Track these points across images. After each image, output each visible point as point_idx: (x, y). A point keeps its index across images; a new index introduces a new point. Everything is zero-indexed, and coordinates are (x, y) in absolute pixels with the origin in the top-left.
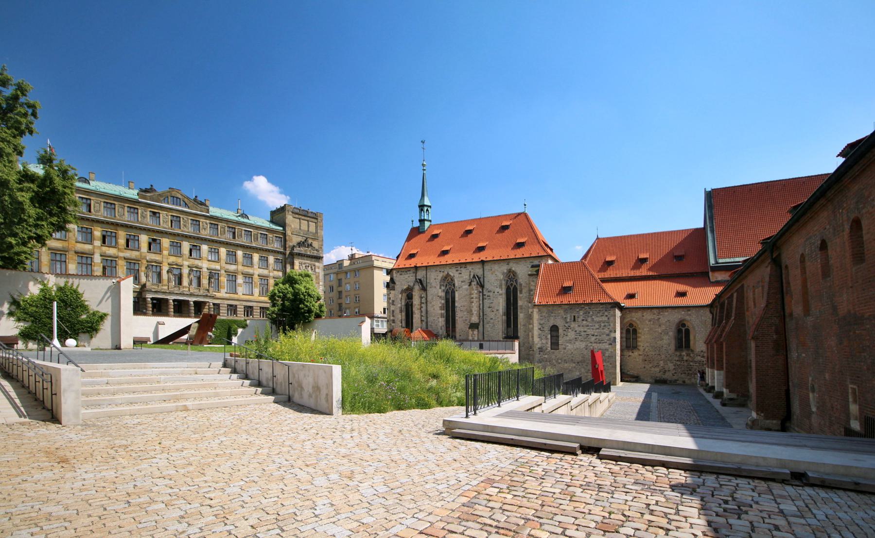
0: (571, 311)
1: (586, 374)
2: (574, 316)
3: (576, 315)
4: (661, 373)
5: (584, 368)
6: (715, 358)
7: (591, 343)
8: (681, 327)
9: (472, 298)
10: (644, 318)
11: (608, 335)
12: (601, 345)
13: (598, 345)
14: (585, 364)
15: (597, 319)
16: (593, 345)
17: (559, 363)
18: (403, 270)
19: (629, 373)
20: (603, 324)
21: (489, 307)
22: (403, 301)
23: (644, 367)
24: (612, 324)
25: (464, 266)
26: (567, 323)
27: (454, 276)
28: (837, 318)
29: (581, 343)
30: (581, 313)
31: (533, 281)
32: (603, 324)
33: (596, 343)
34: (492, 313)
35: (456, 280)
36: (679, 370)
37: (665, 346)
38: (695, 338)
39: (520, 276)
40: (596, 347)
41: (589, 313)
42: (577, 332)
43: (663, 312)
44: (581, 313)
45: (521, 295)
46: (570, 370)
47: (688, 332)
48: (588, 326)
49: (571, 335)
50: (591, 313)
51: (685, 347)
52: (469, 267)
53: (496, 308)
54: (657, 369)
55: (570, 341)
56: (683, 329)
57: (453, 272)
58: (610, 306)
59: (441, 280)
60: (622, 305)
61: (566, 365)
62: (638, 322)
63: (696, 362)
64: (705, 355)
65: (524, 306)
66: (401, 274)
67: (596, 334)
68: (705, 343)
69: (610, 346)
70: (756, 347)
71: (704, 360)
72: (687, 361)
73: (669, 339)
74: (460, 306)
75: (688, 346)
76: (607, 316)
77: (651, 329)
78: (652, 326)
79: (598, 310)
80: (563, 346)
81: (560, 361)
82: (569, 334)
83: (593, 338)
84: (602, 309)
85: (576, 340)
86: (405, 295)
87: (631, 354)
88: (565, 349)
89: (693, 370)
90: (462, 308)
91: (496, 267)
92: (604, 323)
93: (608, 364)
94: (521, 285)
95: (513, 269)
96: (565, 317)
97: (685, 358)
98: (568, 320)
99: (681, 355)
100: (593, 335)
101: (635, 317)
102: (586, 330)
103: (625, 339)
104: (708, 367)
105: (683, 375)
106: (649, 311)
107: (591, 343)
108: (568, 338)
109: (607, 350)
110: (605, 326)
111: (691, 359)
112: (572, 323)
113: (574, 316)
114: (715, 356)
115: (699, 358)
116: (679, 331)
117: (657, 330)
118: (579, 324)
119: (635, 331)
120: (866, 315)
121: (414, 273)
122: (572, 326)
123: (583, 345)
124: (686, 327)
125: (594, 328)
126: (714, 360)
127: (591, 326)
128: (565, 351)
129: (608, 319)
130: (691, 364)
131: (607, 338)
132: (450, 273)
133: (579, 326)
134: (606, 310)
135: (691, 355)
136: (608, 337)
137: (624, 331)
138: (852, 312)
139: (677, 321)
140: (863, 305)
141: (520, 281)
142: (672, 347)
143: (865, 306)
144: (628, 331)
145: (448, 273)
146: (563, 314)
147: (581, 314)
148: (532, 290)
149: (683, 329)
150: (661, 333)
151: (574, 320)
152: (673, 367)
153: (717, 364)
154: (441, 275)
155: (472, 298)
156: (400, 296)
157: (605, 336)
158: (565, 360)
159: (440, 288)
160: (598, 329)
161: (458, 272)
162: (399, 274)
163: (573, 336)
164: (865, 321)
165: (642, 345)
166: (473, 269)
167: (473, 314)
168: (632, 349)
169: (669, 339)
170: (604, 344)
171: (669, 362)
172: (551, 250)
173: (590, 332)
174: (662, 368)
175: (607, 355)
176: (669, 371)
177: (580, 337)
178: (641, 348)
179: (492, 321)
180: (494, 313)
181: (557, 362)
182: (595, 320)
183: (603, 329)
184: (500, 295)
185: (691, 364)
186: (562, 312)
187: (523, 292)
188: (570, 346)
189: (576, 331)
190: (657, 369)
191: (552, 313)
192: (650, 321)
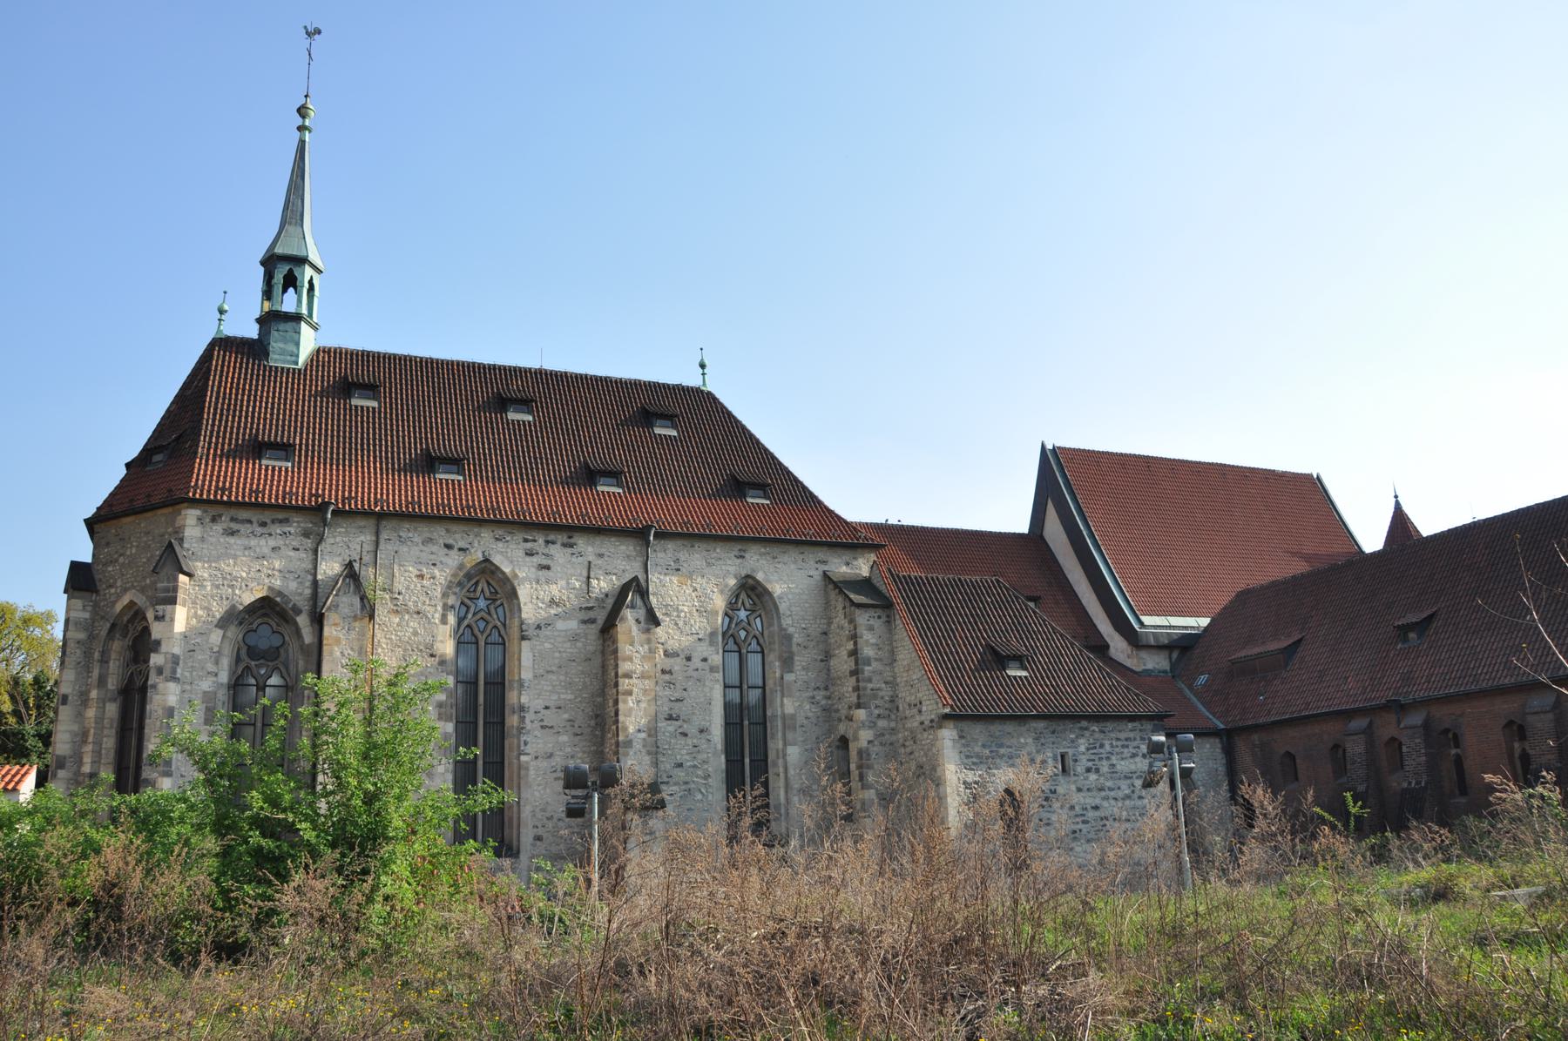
2: (1063, 756)
3: (1070, 752)
9: (628, 676)
18: (243, 514)
21: (670, 718)
22: (225, 662)
25: (561, 538)
27: (516, 576)
29: (1088, 847)
31: (871, 628)
34: (682, 741)
35: (524, 592)
39: (783, 607)
41: (1102, 746)
42: (1077, 808)
45: (789, 677)
48: (1101, 790)
50: (1108, 747)
52: (587, 547)
53: (698, 721)
57: (510, 556)
59: (449, 587)
65: (800, 720)
66: (232, 533)
74: (538, 704)
79: (1123, 735)
82: (1054, 818)
84: (1132, 735)
85: (1075, 839)
86: (234, 632)
90: (551, 718)
91: (695, 557)
94: (788, 638)
95: (760, 576)
102: (1098, 801)
112: (1060, 778)
121: (306, 534)
122: (1060, 790)
127: (1111, 789)
132: (497, 560)
133: (1079, 790)
141: (786, 622)
145: (487, 560)
147: (1082, 749)
148: (868, 662)
151: (1064, 770)
154: (454, 559)
155: (628, 676)
156: (216, 636)
159: (444, 621)
160: (1128, 797)
161: (535, 559)
162: (218, 528)
166: (601, 556)
167: (629, 743)
173: (1111, 808)
179: (680, 774)
180: (689, 741)
182: (1118, 767)
183: (1140, 798)
184: (713, 669)
186: (1030, 740)
187: (800, 661)
189: (1072, 808)
191: (1001, 746)
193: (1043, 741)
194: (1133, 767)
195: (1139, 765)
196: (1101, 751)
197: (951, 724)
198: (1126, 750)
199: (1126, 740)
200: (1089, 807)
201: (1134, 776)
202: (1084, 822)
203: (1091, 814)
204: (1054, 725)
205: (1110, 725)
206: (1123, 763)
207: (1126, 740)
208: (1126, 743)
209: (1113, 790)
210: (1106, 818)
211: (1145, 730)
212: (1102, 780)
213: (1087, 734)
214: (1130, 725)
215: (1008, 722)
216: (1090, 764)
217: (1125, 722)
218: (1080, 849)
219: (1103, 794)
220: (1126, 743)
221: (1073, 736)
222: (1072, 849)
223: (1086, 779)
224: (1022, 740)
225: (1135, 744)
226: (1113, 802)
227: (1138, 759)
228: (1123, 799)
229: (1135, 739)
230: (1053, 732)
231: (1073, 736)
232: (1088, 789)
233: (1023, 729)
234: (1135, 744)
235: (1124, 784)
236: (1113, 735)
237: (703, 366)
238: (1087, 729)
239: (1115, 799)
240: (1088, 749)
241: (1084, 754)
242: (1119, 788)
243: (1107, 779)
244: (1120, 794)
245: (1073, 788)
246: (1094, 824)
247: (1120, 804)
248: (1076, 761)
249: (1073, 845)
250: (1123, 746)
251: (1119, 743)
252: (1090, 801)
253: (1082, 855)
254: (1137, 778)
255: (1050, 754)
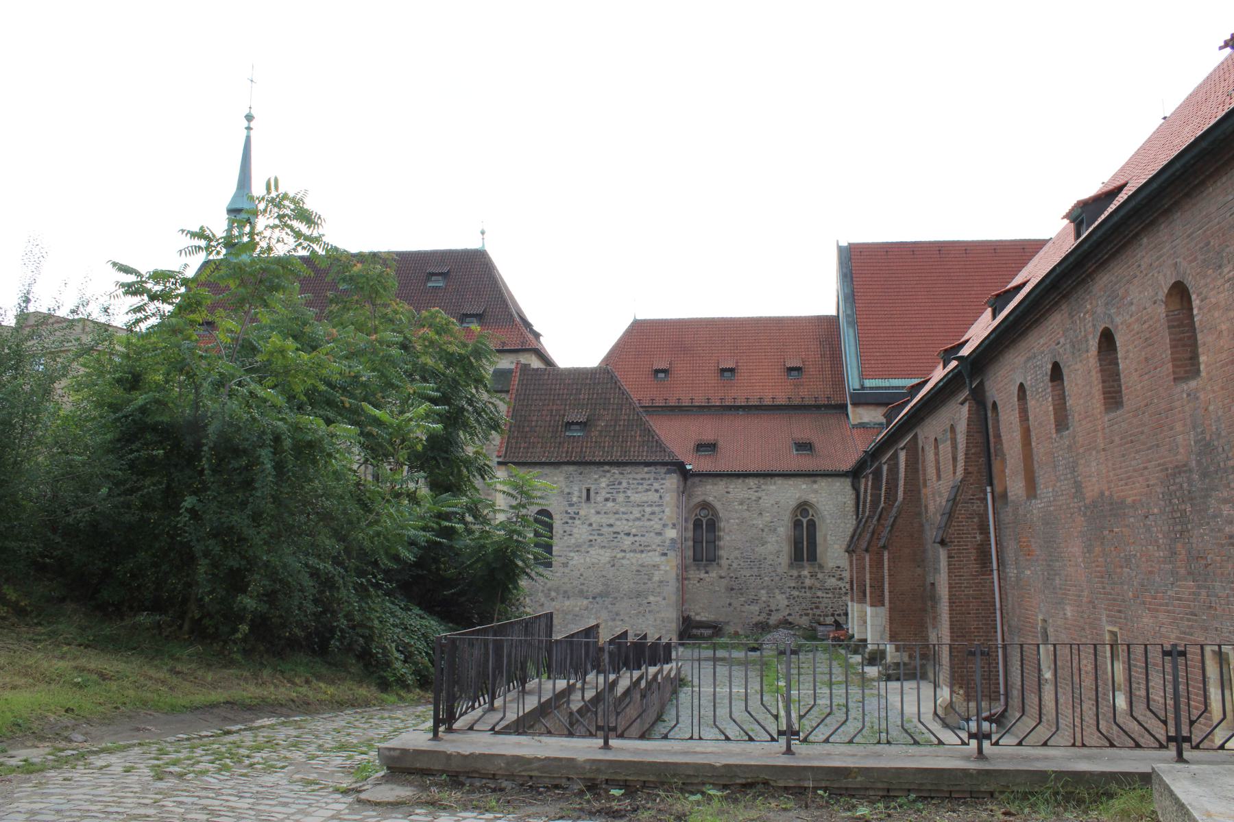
0: (581, 477)
1: (610, 623)
2: (588, 490)
3: (593, 488)
4: (764, 615)
5: (607, 608)
6: (868, 582)
7: (624, 551)
8: (800, 517)
10: (729, 496)
11: (659, 534)
12: (643, 555)
13: (638, 555)
14: (608, 600)
15: (636, 498)
16: (628, 555)
17: (553, 600)
19: (698, 618)
20: (648, 510)
23: (730, 604)
24: (667, 510)
26: (571, 505)
28: (1081, 504)
29: (602, 552)
30: (604, 483)
32: (648, 510)
33: (634, 551)
36: (797, 609)
37: (771, 557)
38: (825, 540)
40: (634, 561)
41: (620, 483)
42: (594, 525)
43: (766, 484)
44: (604, 483)
46: (577, 616)
47: (812, 525)
48: (615, 513)
49: (581, 532)
50: (624, 484)
51: (808, 560)
54: (755, 608)
55: (577, 548)
56: (805, 521)
58: (663, 470)
60: (689, 467)
61: (567, 603)
62: (718, 506)
63: (827, 590)
64: (846, 575)
67: (634, 531)
68: (846, 551)
69: (663, 558)
70: (949, 557)
71: (841, 584)
72: (810, 588)
73: (777, 541)
75: (813, 557)
76: (657, 491)
77: (743, 520)
78: (746, 514)
79: (639, 476)
80: (563, 560)
81: (553, 594)
82: (575, 530)
83: (628, 541)
84: (647, 476)
85: (591, 546)
87: (703, 575)
88: (565, 565)
89: (822, 606)
92: (651, 506)
93: (658, 599)
96: (567, 490)
97: (808, 582)
98: (575, 499)
99: (800, 576)
100: (628, 534)
101: (712, 492)
102: (611, 521)
103: (691, 543)
104: (852, 600)
105: (804, 617)
106: (740, 481)
107: (624, 551)
108: (573, 541)
109: (657, 567)
110: (653, 513)
111: (818, 585)
112: (583, 504)
113: (588, 490)
114: (868, 576)
115: (832, 582)
116: (797, 524)
117: (755, 522)
118: (599, 508)
119: (713, 525)
120: (1129, 500)
122: (582, 513)
123: (605, 556)
124: (810, 517)
125: (632, 517)
126: (865, 586)
127: (623, 513)
128: (567, 570)
129: (661, 497)
130: (820, 594)
131: (658, 540)
133: (598, 513)
134: (656, 479)
135: (820, 576)
136: (660, 537)
137: (691, 526)
138: (1107, 493)
139: (793, 504)
140: (1123, 482)
142: (784, 559)
143: (1126, 484)
144: (697, 525)
146: (563, 484)
147: (603, 485)
149: (805, 521)
150: (763, 530)
152: (786, 603)
153: (871, 593)
157: (652, 534)
158: (565, 592)
160: (639, 519)
163: (586, 537)
164: (1126, 511)
165: (725, 557)
168: (706, 566)
169: (777, 541)
170: (650, 554)
171: (777, 591)
172: (537, 335)
173: (621, 526)
174: (764, 605)
175: (656, 578)
176: (777, 610)
177: (599, 539)
178: (724, 562)
181: (547, 596)
182: (632, 499)
185: (820, 594)
188: (576, 559)
189: (591, 525)
190: (755, 608)
192: (741, 503)
193: (571, 479)
194: (645, 499)
195: (651, 497)
196: (618, 487)
197: (503, 468)
198: (640, 487)
199: (642, 479)
200: (604, 525)
201: (646, 505)
202: (599, 535)
203: (605, 530)
204: (581, 469)
205: (628, 469)
206: (636, 495)
207: (642, 479)
208: (641, 481)
209: (626, 513)
210: (618, 533)
211: (659, 473)
212: (617, 507)
213: (608, 475)
214: (646, 469)
215: (546, 467)
216: (608, 496)
217: (642, 467)
218: (594, 552)
219: (617, 516)
220: (641, 481)
221: (596, 476)
222: (588, 552)
223: (605, 505)
224: (556, 479)
225: (649, 482)
226: (625, 522)
227: (649, 493)
228: (634, 520)
229: (649, 479)
230: (581, 474)
231: (596, 476)
232: (605, 513)
233: (557, 471)
234: (649, 482)
235: (636, 513)
236: (630, 476)
237: (483, 233)
238: (608, 471)
239: (627, 520)
240: (608, 485)
241: (604, 488)
242: (631, 513)
243: (622, 507)
244: (632, 517)
245: (593, 511)
246: (607, 536)
247: (630, 524)
248: (597, 493)
249: (589, 549)
250: (638, 484)
251: (635, 482)
252: (604, 520)
253: (596, 556)
254: (648, 506)
255: (576, 489)
